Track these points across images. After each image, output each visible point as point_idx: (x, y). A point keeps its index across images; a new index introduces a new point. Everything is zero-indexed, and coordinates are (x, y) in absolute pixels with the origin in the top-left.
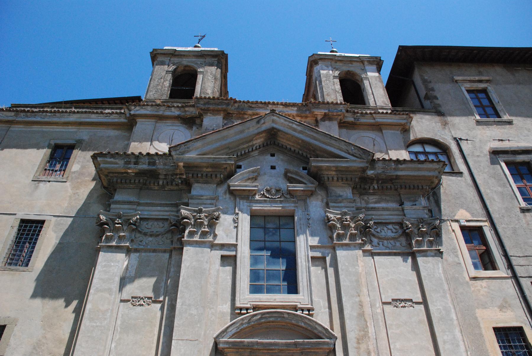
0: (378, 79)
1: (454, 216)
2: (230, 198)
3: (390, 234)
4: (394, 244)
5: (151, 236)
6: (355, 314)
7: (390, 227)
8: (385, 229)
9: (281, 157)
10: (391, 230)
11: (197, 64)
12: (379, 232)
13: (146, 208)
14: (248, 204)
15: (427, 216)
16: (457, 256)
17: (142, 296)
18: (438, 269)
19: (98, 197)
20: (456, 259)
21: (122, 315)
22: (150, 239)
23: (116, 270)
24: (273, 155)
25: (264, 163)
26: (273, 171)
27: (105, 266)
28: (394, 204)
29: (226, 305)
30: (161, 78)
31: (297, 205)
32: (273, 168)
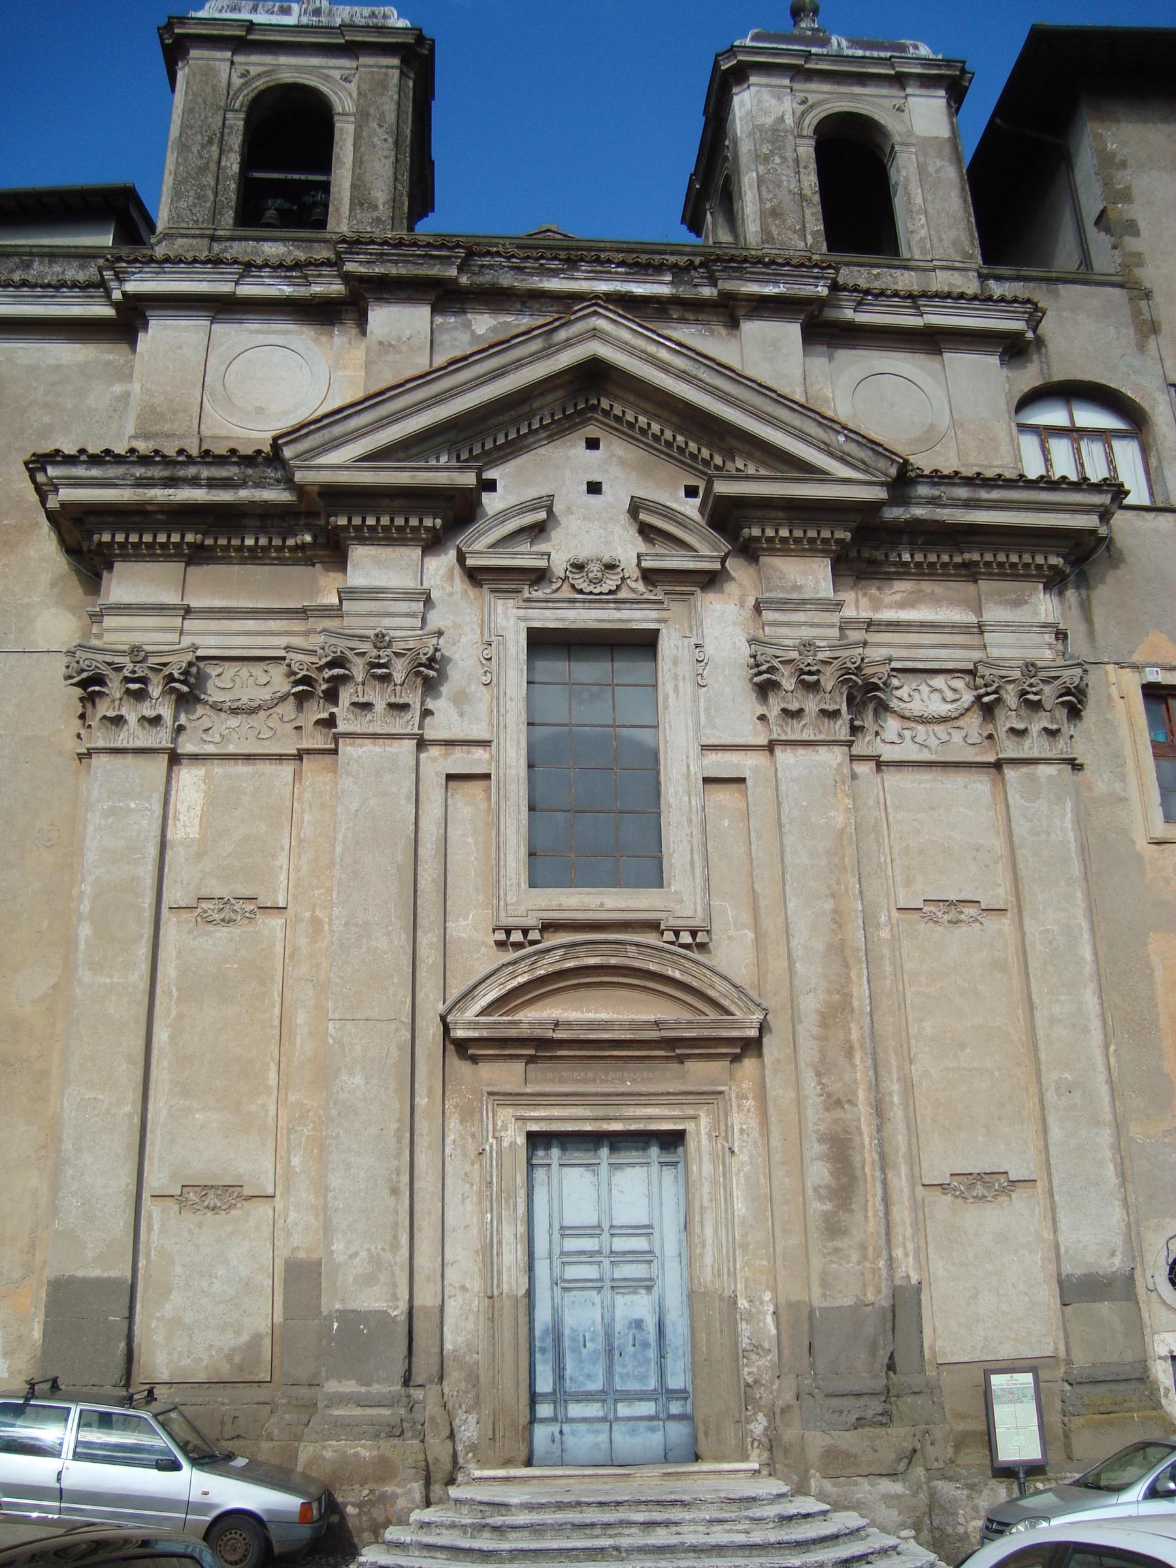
0: (947, 150)
1: (1131, 653)
2: (465, 592)
3: (939, 708)
4: (945, 737)
5: (235, 711)
6: (820, 946)
7: (939, 682)
8: (924, 688)
9: (620, 452)
10: (940, 691)
11: (327, 78)
12: (906, 698)
13: (213, 625)
14: (521, 612)
15: (1048, 654)
16: (1123, 778)
17: (226, 894)
18: (1064, 816)
19: (53, 585)
20: (1118, 786)
21: (179, 953)
22: (234, 722)
23: (145, 822)
24: (593, 444)
25: (568, 473)
26: (593, 499)
27: (112, 812)
28: (956, 610)
29: (466, 919)
30: (211, 141)
31: (665, 614)
32: (594, 488)
